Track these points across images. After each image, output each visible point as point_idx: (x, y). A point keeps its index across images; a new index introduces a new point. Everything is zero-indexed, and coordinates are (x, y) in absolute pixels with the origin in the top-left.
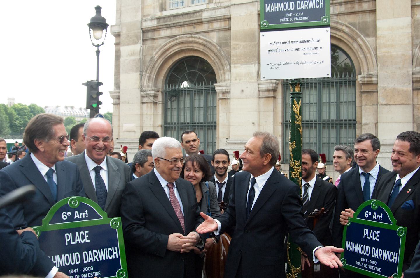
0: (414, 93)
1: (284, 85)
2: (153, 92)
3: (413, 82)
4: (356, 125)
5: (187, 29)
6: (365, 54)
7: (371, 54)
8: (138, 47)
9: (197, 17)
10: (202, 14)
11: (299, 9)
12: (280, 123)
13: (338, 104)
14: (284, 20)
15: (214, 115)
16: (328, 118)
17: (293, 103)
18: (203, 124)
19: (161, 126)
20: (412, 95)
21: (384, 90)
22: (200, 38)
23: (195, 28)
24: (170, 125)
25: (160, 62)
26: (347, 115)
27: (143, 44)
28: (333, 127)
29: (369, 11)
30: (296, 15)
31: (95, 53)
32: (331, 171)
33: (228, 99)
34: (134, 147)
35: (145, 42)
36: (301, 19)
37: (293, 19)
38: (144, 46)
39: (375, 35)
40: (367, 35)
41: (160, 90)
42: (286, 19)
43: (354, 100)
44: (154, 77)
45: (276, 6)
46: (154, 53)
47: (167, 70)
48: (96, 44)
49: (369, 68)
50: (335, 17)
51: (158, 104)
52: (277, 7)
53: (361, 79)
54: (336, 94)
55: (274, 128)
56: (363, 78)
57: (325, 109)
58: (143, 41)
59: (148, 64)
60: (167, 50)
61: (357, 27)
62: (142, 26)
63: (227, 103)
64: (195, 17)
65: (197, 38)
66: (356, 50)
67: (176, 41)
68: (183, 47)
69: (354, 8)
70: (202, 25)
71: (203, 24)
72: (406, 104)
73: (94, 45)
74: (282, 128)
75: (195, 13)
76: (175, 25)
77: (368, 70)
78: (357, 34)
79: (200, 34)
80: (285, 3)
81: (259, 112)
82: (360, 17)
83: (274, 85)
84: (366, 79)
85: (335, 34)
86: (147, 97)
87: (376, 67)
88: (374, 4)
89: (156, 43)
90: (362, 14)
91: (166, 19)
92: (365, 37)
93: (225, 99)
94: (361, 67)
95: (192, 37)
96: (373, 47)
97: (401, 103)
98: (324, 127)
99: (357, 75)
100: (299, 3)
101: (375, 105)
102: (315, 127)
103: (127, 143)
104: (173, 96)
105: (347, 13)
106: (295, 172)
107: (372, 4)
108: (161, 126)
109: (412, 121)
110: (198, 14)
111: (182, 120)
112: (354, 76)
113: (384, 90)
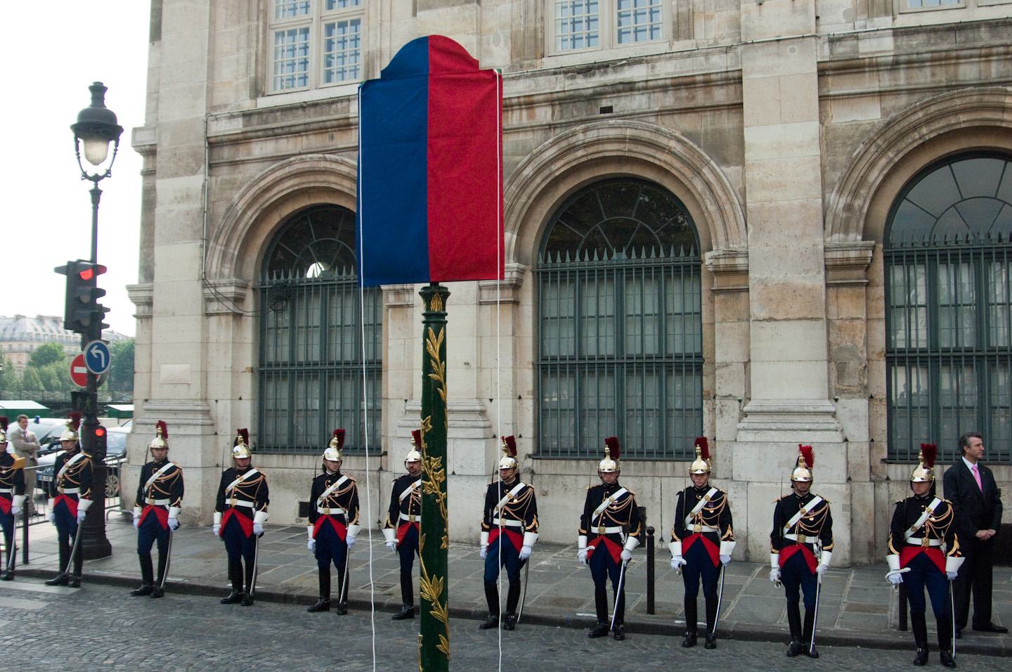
0: (830, 294)
1: (538, 273)
2: (232, 289)
3: (827, 268)
4: (702, 366)
5: (314, 141)
6: (721, 204)
7: (732, 203)
8: (197, 181)
9: (336, 112)
10: (348, 106)
12: (528, 363)
13: (663, 318)
15: (376, 343)
16: (638, 352)
17: (426, 335)
18: (350, 366)
19: (252, 370)
20: (824, 297)
21: (762, 286)
22: (342, 163)
23: (332, 138)
24: (274, 368)
25: (251, 218)
26: (684, 343)
27: (209, 175)
28: (650, 372)
29: (728, 105)
31: (89, 197)
32: (647, 474)
33: (408, 306)
34: (186, 422)
35: (216, 169)
38: (214, 178)
39: (741, 160)
40: (724, 161)
41: (251, 284)
43: (696, 310)
44: (236, 253)
46: (236, 196)
47: (267, 237)
48: (91, 174)
49: (729, 236)
50: (652, 119)
51: (244, 318)
53: (711, 261)
54: (656, 297)
55: (515, 374)
56: (716, 258)
57: (632, 330)
58: (211, 166)
59: (220, 221)
60: (267, 190)
61: (702, 141)
62: (209, 132)
63: (407, 316)
64: (332, 112)
65: (336, 162)
66: (700, 194)
67: (287, 170)
68: (303, 183)
69: (694, 98)
70: (349, 132)
71: (351, 129)
72: (812, 319)
73: (85, 176)
74: (534, 374)
75: (333, 103)
76: (287, 130)
77: (727, 240)
78: (701, 157)
79: (344, 153)
81: (480, 338)
82: (709, 118)
83: (515, 275)
84: (722, 262)
85: (652, 156)
86: (218, 300)
87: (745, 235)
88: (738, 91)
89: (240, 172)
90: (712, 113)
91: (264, 116)
92: (718, 165)
93: (402, 306)
94: (712, 234)
95: (325, 160)
96: (737, 189)
97: (801, 316)
98: (630, 372)
99: (704, 253)
101: (743, 320)
102: (611, 373)
103: (170, 410)
104: (279, 299)
105: (680, 109)
106: (430, 483)
107: (733, 91)
108: (252, 370)
109: (825, 356)
110: (339, 105)
111: (301, 358)
112: (698, 253)
113: (762, 286)
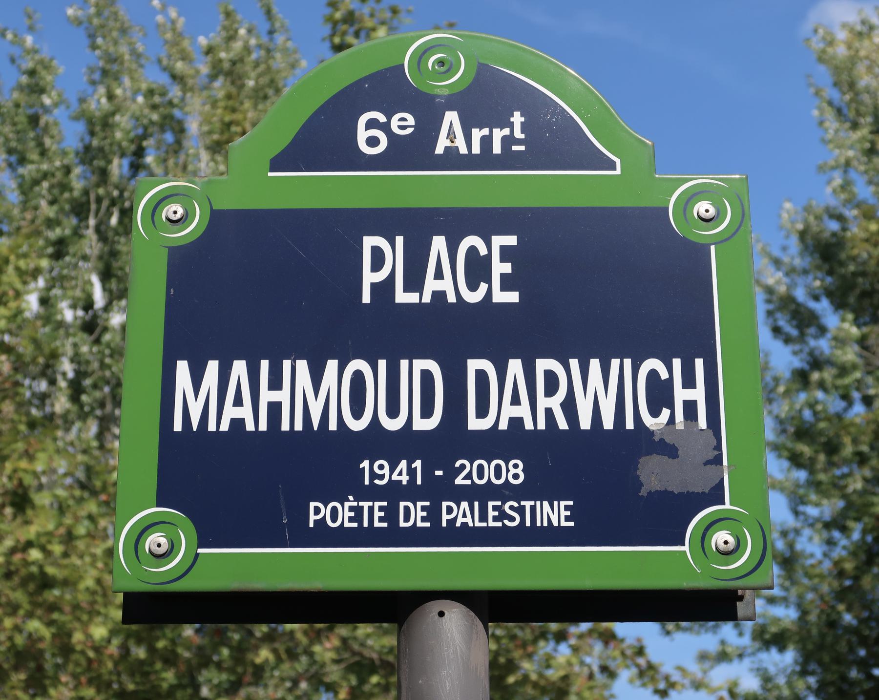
11: (485, 424)
14: (345, 515)
30: (459, 481)
36: (502, 516)
37: (433, 514)
42: (358, 511)
45: (275, 384)
52: (282, 396)
80: (358, 364)
100: (482, 376)
